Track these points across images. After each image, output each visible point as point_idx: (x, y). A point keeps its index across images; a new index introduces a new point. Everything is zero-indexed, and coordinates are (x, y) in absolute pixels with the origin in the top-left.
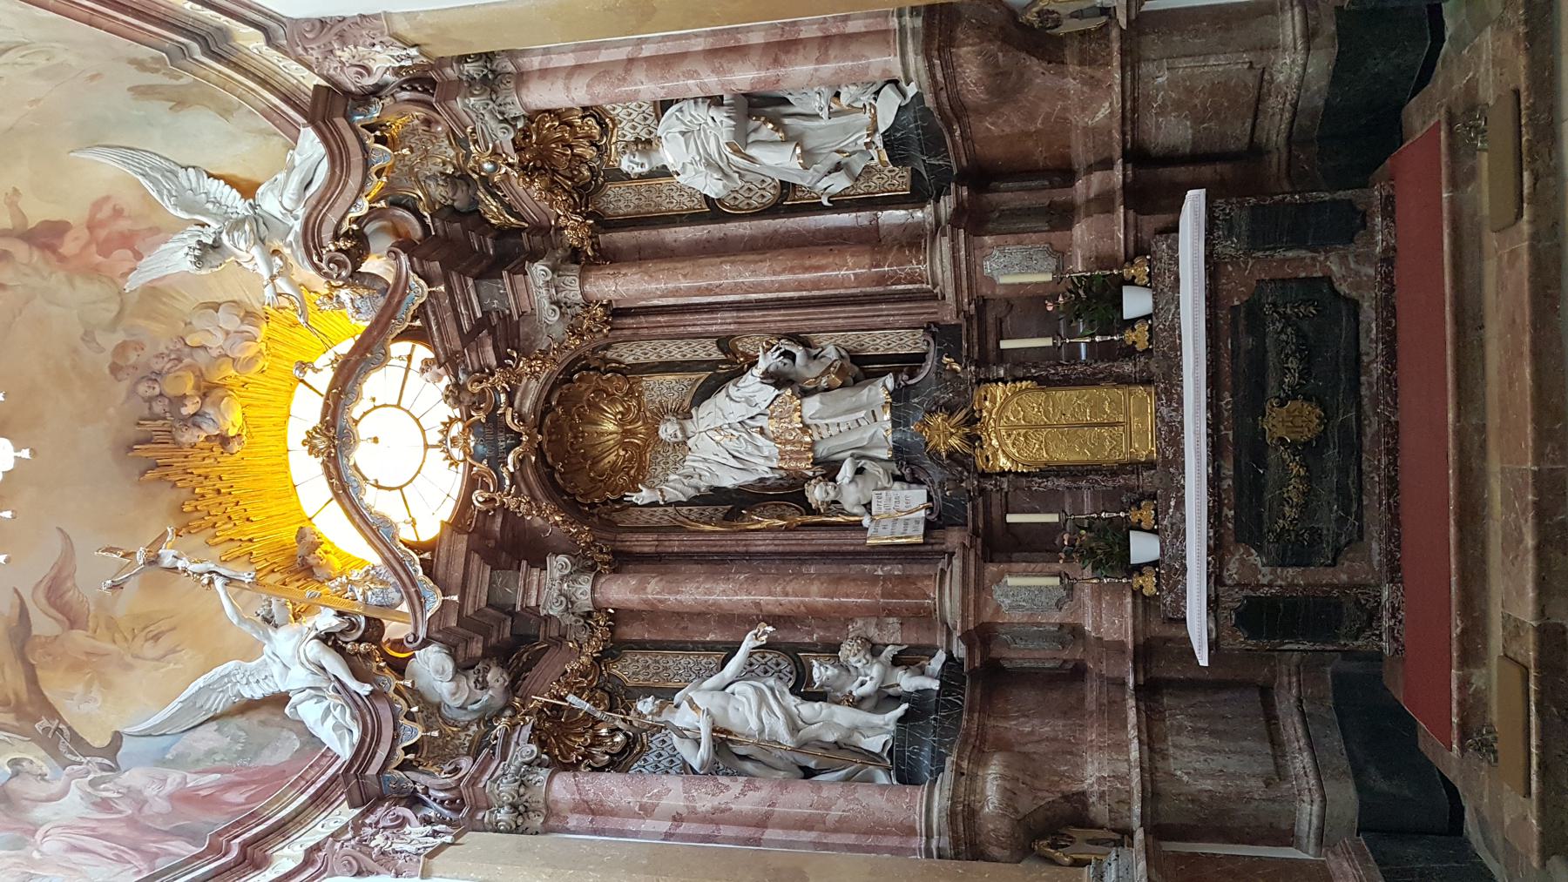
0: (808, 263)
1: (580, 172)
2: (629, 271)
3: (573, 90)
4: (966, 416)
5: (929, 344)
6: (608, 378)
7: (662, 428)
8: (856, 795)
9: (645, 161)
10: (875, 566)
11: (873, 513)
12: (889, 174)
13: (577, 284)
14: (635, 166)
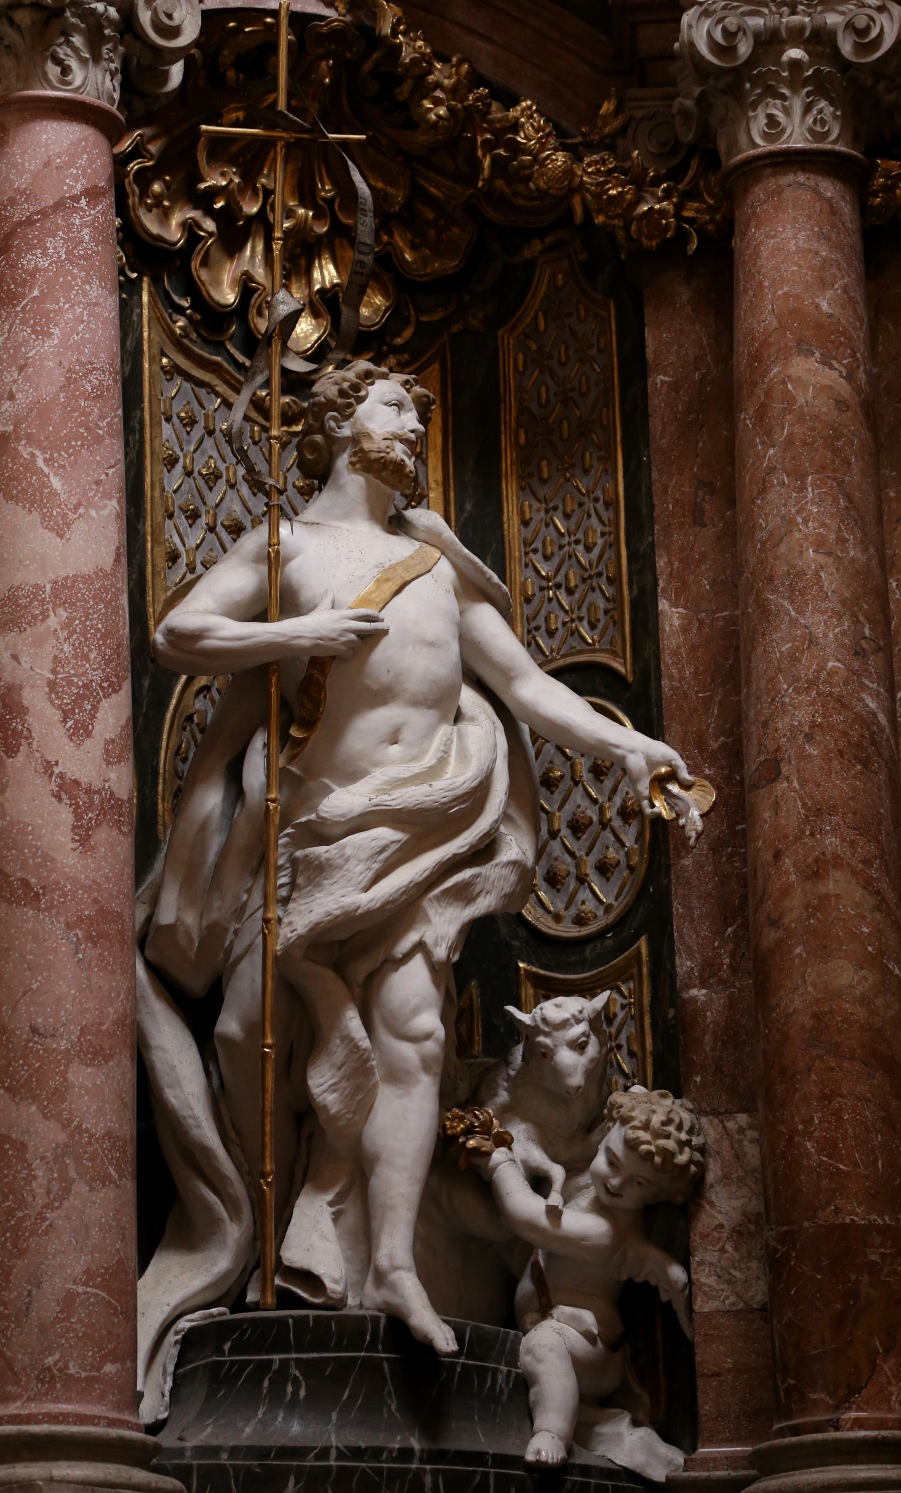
8: (81, 1188)
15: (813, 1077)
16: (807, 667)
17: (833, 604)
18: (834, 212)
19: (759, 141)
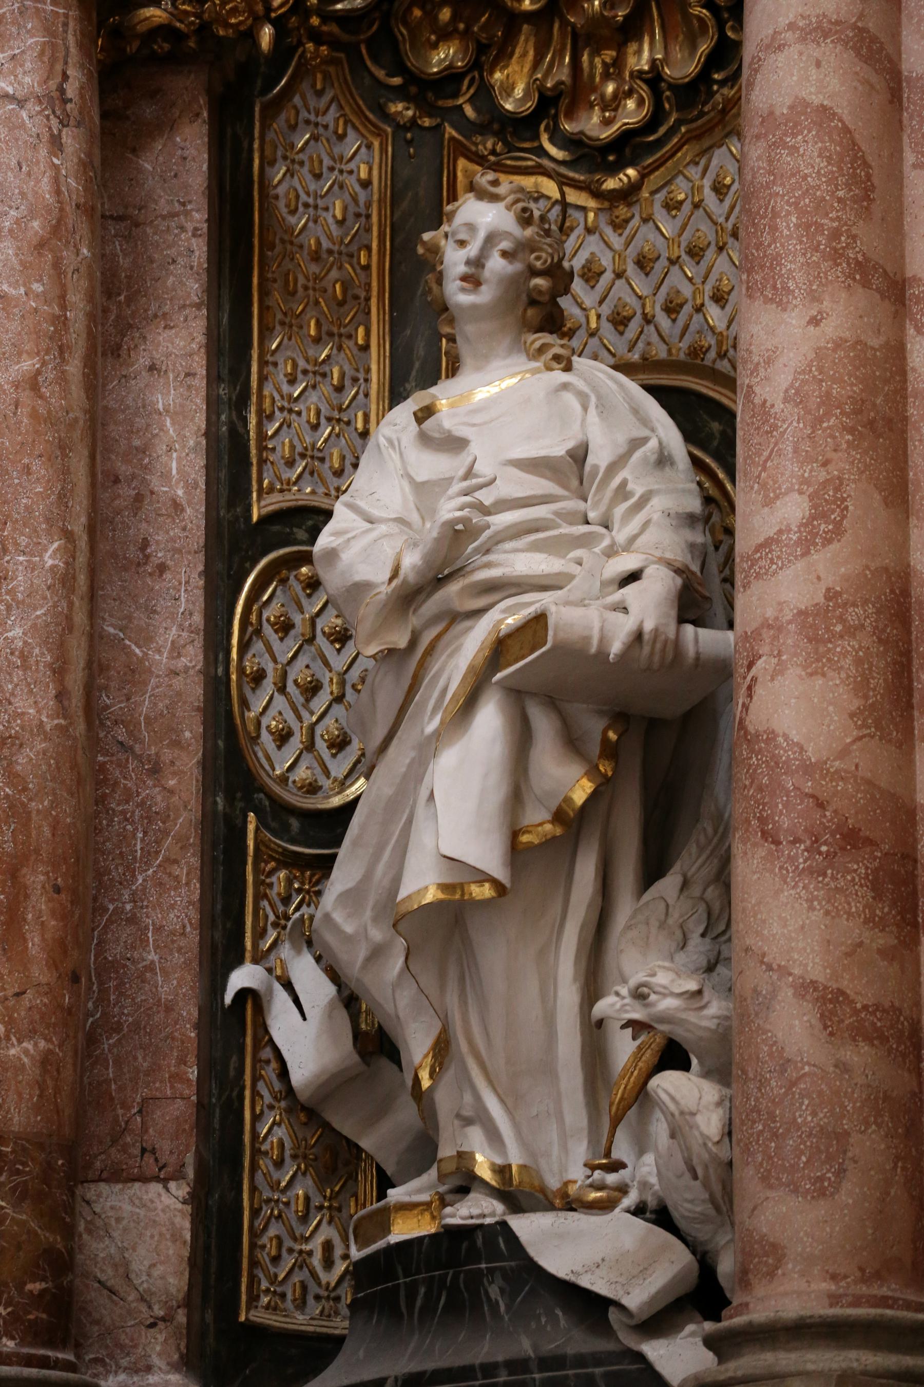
1: (445, 35)
2: (68, 162)
3: (815, 52)
9: (485, 296)
12: (315, 1246)
14: (472, 250)
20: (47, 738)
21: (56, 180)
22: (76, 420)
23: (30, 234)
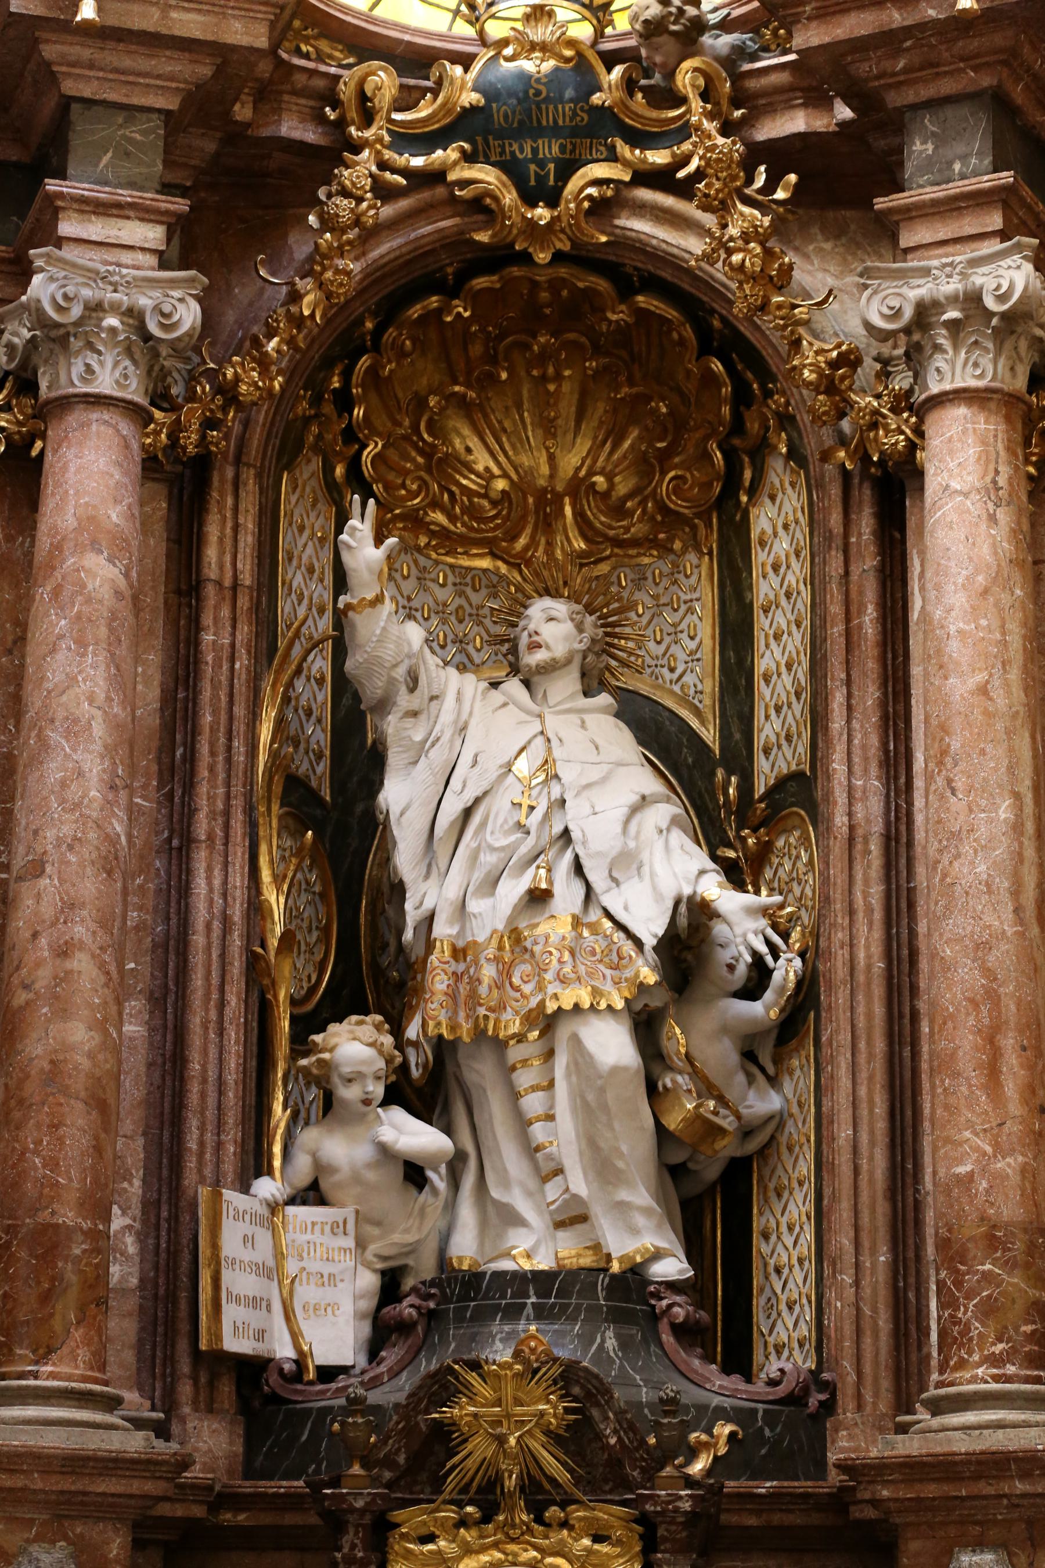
0: (1009, 1042)
4: (552, 1480)
5: (773, 1383)
6: (707, 456)
7: (560, 607)
10: (136, 1210)
11: (291, 1210)
13: (973, 383)
15: (46, 1109)
16: (74, 792)
17: (97, 747)
18: (127, 446)
19: (76, 382)
20: (1009, 942)
21: (994, 545)
22: (1017, 712)
23: (977, 585)
